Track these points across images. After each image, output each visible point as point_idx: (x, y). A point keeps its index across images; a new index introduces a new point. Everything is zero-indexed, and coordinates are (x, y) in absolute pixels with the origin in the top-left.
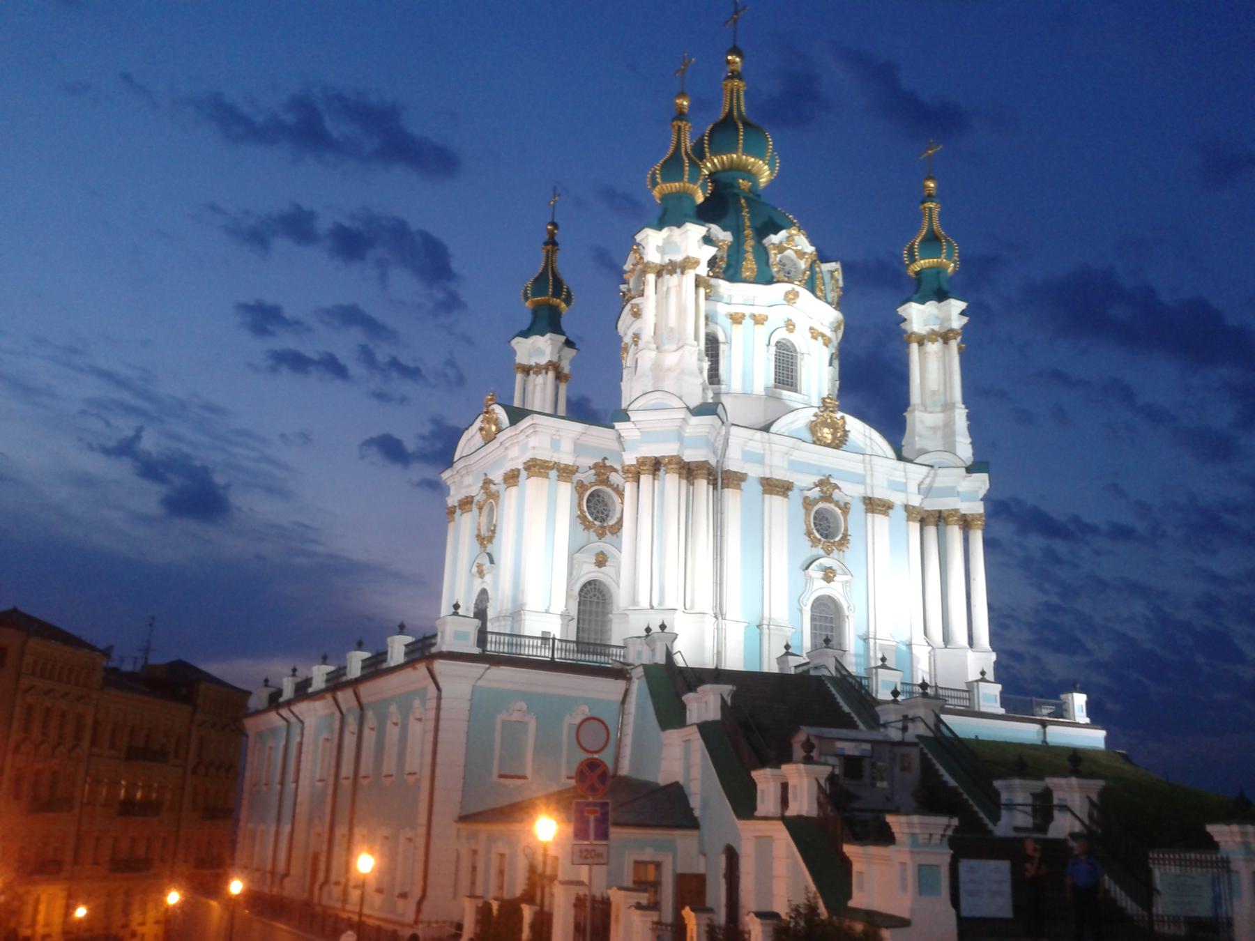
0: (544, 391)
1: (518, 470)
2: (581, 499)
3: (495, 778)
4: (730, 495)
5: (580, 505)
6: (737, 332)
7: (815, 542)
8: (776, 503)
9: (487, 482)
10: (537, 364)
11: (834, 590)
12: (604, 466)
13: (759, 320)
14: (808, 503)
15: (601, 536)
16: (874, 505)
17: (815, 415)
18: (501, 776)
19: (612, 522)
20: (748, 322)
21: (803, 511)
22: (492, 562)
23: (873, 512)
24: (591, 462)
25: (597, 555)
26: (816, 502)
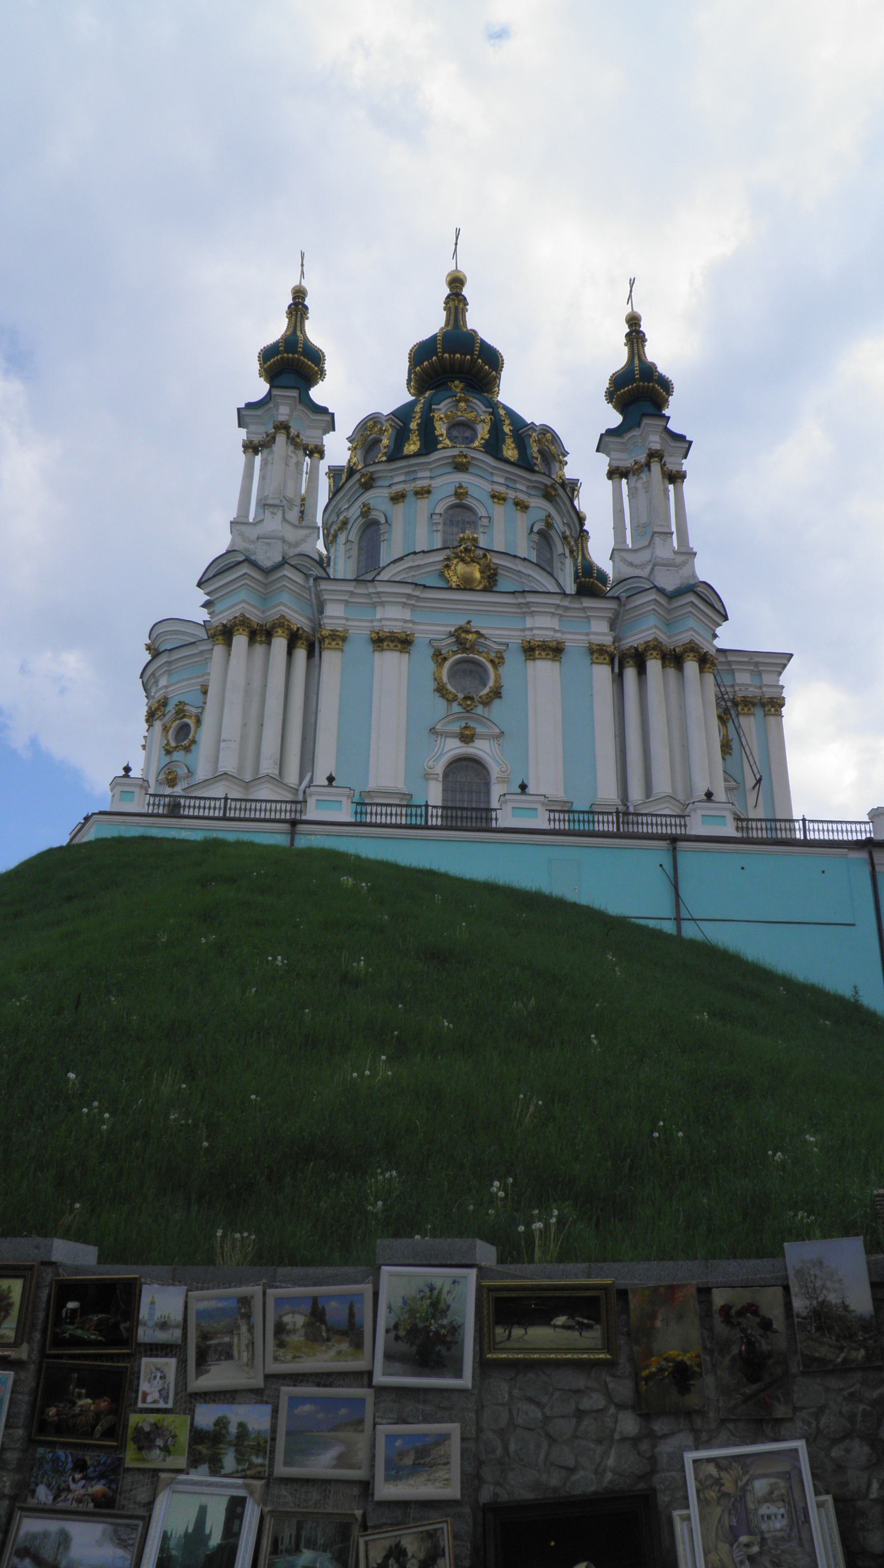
6: (398, 512)
14: (439, 657)
23: (534, 659)
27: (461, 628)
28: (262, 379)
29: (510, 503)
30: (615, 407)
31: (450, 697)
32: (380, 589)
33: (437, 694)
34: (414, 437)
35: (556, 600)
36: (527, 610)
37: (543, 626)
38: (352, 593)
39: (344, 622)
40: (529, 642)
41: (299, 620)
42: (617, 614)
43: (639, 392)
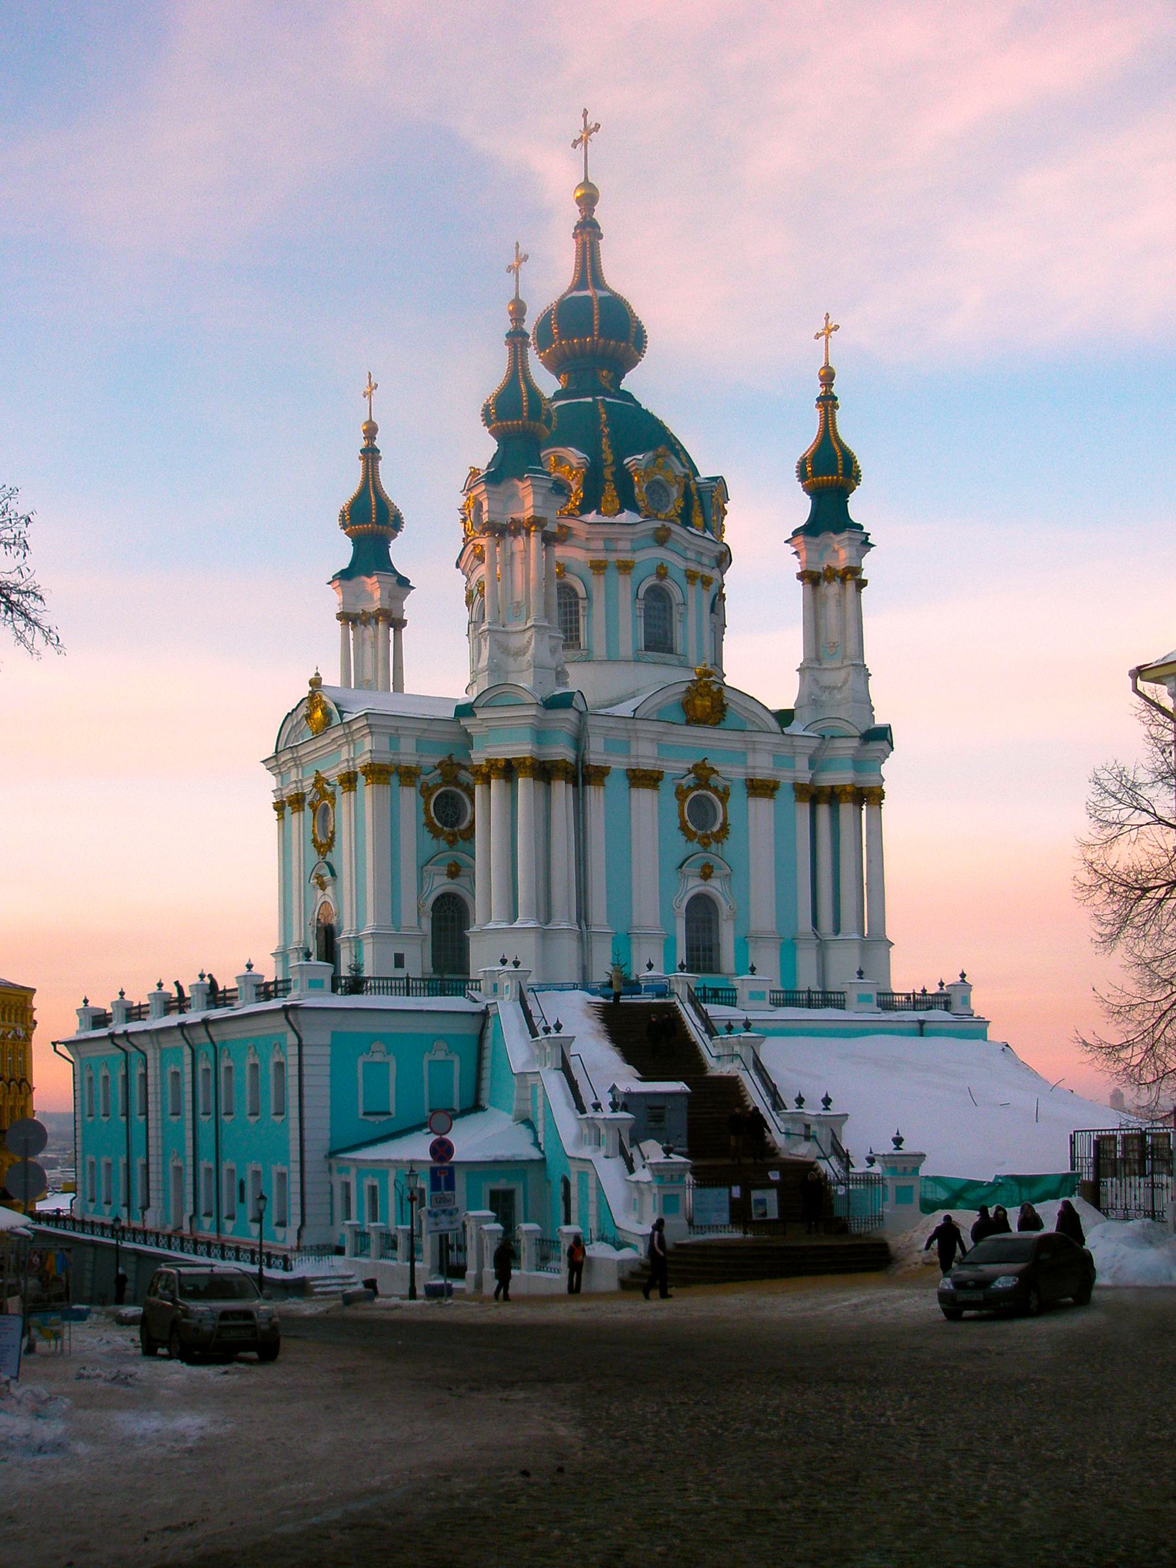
0: (374, 646)
1: (356, 773)
2: (427, 804)
3: (361, 1116)
4: (591, 790)
5: (427, 811)
7: (689, 835)
8: (644, 798)
9: (319, 780)
10: (364, 612)
11: (714, 887)
12: (452, 764)
13: (625, 567)
14: (681, 793)
15: (452, 843)
17: (688, 690)
18: (365, 1114)
19: (464, 825)
20: (612, 573)
21: (675, 802)
22: (333, 873)
24: (439, 760)
25: (450, 865)
26: (691, 789)
29: (698, 582)
30: (805, 489)
32: (637, 727)
33: (680, 833)
40: (752, 780)
41: (569, 755)
42: (817, 749)
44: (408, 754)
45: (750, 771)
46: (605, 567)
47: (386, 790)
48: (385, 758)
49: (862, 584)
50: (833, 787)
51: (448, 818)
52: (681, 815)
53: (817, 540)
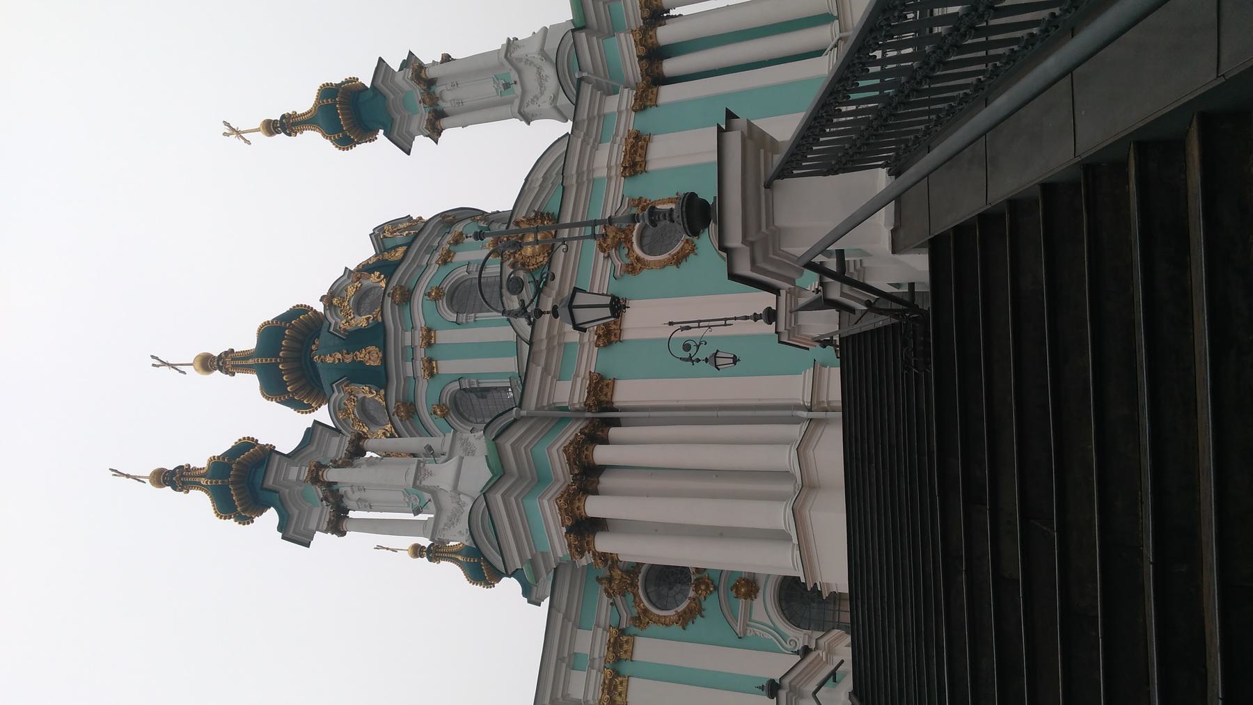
5: (666, 623)
12: (610, 580)
14: (634, 268)
16: (634, 164)
24: (605, 598)
27: (600, 246)
28: (256, 519)
31: (688, 247)
32: (544, 336)
33: (684, 263)
34: (361, 356)
35: (578, 143)
36: (586, 177)
37: (607, 157)
38: (546, 370)
39: (579, 380)
40: (625, 168)
41: (571, 431)
42: (598, 86)
43: (350, 113)
44: (590, 643)
45: (613, 173)
46: (430, 361)
47: (634, 683)
48: (597, 678)
49: (447, 58)
50: (640, 58)
51: (671, 591)
52: (663, 265)
53: (398, 117)
